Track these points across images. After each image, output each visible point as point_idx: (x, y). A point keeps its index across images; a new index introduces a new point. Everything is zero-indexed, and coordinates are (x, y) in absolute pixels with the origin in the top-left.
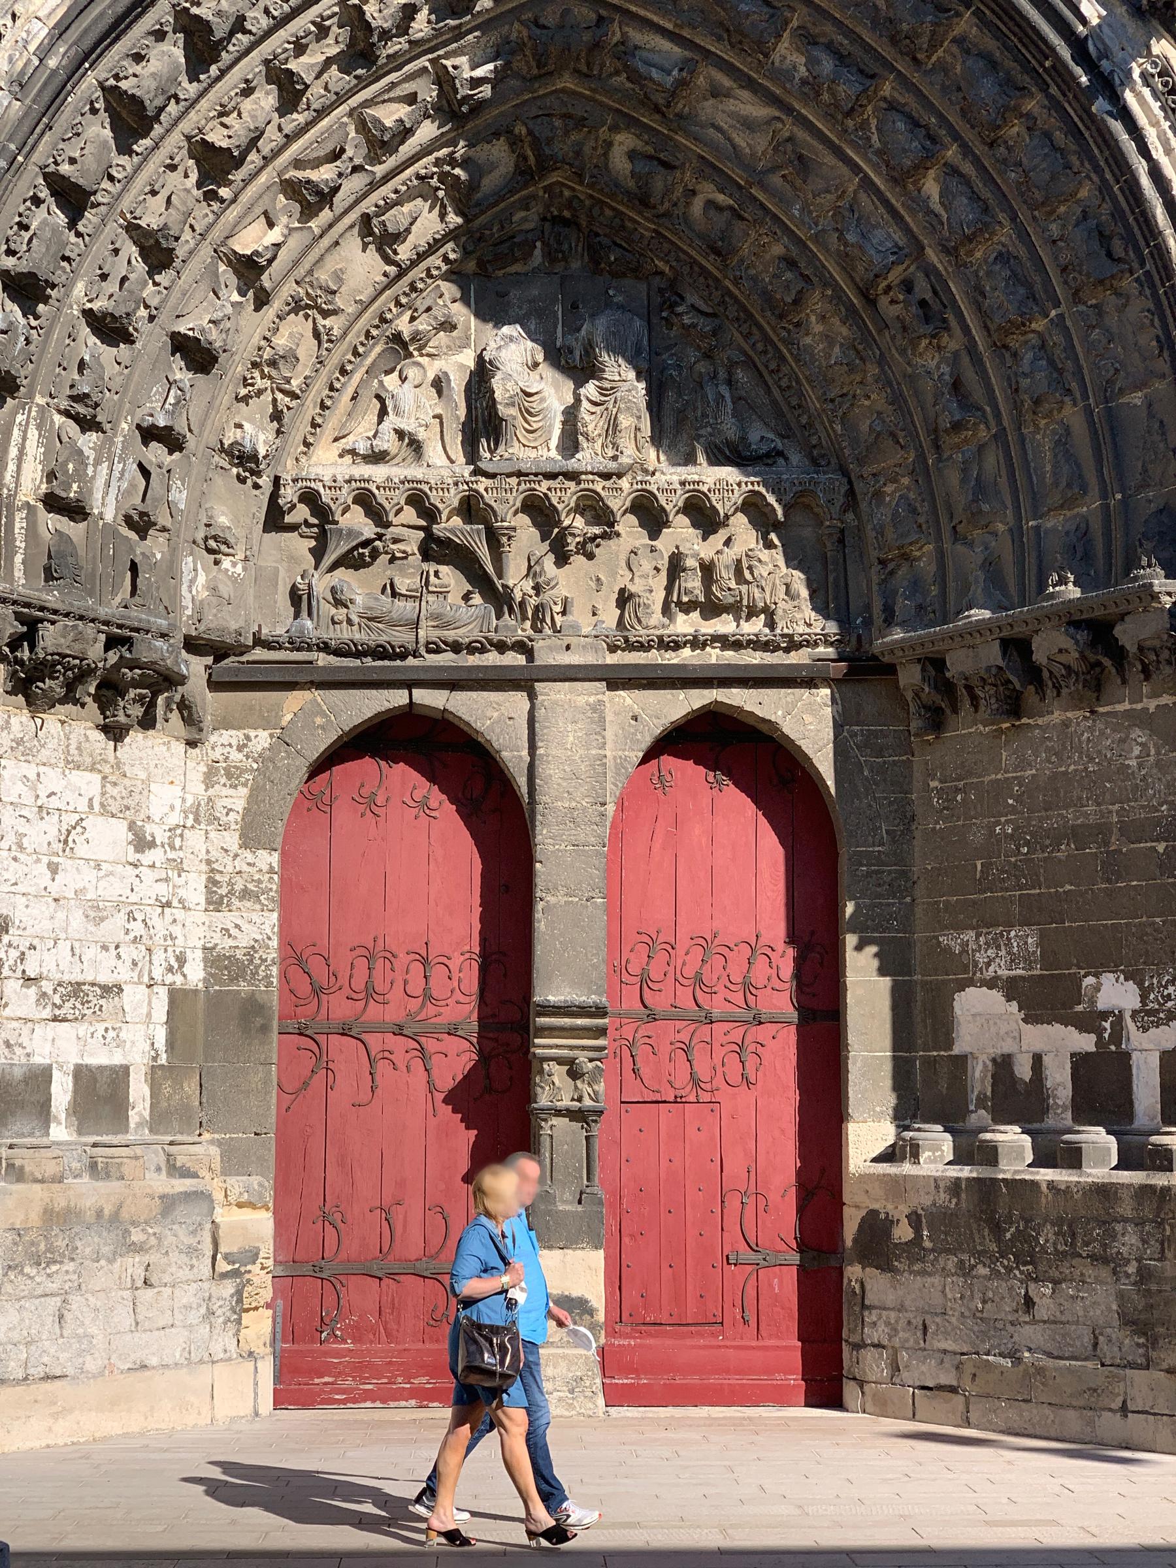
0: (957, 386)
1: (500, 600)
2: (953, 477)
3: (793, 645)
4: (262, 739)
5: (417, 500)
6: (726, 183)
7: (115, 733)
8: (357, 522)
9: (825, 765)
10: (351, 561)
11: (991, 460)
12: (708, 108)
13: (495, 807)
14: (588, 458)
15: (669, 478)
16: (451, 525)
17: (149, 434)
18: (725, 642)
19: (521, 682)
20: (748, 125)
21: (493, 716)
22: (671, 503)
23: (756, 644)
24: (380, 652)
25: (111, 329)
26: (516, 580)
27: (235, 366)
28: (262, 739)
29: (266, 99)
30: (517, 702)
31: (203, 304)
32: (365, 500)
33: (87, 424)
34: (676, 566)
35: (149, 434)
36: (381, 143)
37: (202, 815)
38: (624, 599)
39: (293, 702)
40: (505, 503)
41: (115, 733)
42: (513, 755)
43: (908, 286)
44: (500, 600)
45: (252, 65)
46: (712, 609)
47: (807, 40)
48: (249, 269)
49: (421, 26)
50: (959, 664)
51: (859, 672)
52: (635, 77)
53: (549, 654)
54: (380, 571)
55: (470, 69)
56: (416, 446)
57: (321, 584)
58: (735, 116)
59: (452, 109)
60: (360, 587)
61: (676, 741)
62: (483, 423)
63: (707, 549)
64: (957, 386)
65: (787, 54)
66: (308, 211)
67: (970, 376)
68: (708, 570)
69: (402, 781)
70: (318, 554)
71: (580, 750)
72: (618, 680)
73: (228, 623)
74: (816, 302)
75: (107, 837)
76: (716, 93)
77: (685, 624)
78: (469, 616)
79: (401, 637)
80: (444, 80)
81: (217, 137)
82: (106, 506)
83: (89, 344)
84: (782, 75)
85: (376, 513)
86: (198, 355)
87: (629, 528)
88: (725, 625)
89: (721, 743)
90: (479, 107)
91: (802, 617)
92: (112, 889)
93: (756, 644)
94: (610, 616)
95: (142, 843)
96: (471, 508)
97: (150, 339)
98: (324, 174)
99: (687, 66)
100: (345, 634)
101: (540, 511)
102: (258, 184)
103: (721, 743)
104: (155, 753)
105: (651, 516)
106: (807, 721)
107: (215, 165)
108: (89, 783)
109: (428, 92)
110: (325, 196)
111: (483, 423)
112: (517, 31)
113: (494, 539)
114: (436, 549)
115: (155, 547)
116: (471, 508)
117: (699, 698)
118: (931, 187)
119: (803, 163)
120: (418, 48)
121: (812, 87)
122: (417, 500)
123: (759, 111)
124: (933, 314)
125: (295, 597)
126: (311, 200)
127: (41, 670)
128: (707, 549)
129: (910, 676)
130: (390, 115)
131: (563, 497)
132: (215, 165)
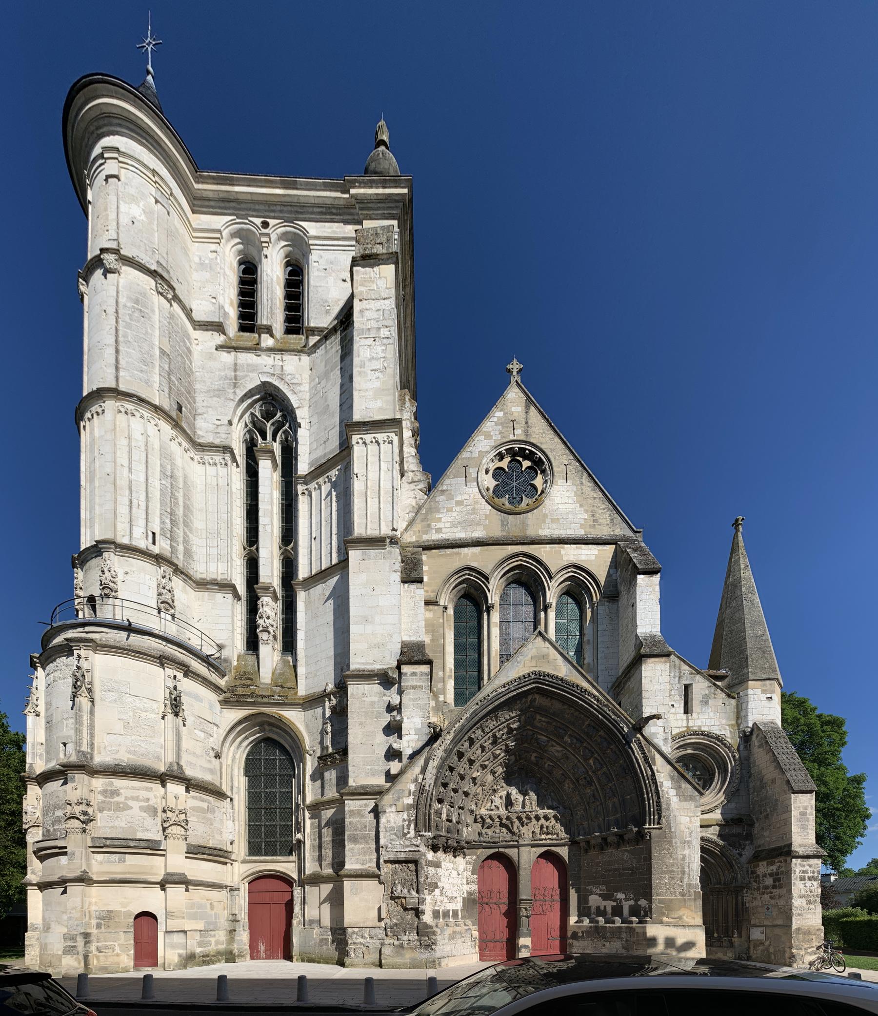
0: (594, 795)
1: (513, 833)
2: (592, 811)
3: (562, 839)
4: (474, 857)
5: (499, 817)
6: (552, 761)
7: (455, 857)
8: (488, 821)
9: (567, 859)
10: (488, 828)
11: (599, 808)
12: (551, 749)
13: (511, 868)
14: (527, 809)
15: (541, 812)
16: (504, 821)
17: (460, 808)
18: (550, 839)
19: (517, 847)
20: (558, 751)
21: (512, 853)
22: (541, 816)
23: (556, 839)
24: (493, 843)
25: (455, 791)
26: (515, 830)
27: (471, 796)
28: (474, 857)
29: (480, 751)
30: (516, 850)
31: (467, 786)
32: (491, 817)
33: (452, 807)
34: (542, 827)
35: (460, 808)
36: (495, 757)
37: (466, 870)
38: (533, 832)
39: (479, 851)
40: (514, 817)
41: (455, 857)
42: (516, 859)
43: (585, 778)
44: (513, 833)
45: (478, 745)
46: (548, 834)
47: (571, 736)
48: (474, 779)
49: (504, 737)
50: (593, 842)
51: (573, 844)
52: (538, 743)
53: (521, 842)
54: (493, 829)
55: (512, 744)
56: (498, 808)
57: (484, 831)
58: (556, 750)
59: (507, 751)
60: (490, 832)
61: (541, 856)
62: (509, 803)
63: (547, 824)
64: (594, 795)
65: (567, 739)
66: (484, 769)
67: (596, 793)
68: (547, 827)
69: (495, 863)
70: (483, 827)
71: (526, 857)
72: (533, 846)
73: (470, 838)
74: (567, 781)
75: (454, 873)
76: (552, 746)
77: (543, 836)
78: (508, 836)
79: (497, 840)
80: (507, 745)
81: (472, 758)
82: (454, 821)
83: (452, 794)
84: (565, 743)
85: (492, 820)
86: (466, 794)
87: (534, 821)
88: (550, 836)
89: (549, 856)
90: (511, 750)
91: (563, 835)
92: (455, 882)
93: (556, 839)
94: (531, 835)
95: (459, 875)
96: (508, 818)
97: (460, 792)
98: (487, 763)
99: (548, 741)
100: (488, 840)
101: (519, 818)
102: (477, 765)
103: (549, 856)
104: (460, 859)
105: (537, 818)
106: (564, 852)
107: (471, 762)
108: (452, 865)
109: (504, 748)
110: (486, 766)
111: (509, 803)
112: (519, 736)
113: (512, 823)
114: (502, 825)
115: (460, 826)
116: (508, 818)
117: (546, 849)
118: (591, 762)
119: (567, 758)
120: (504, 740)
121: (570, 745)
122: (499, 817)
123: (560, 749)
124: (590, 783)
125: (479, 834)
126: (484, 767)
127: (448, 847)
128: (547, 824)
129: (583, 844)
130: (498, 752)
131: (523, 816)
132: (471, 762)
